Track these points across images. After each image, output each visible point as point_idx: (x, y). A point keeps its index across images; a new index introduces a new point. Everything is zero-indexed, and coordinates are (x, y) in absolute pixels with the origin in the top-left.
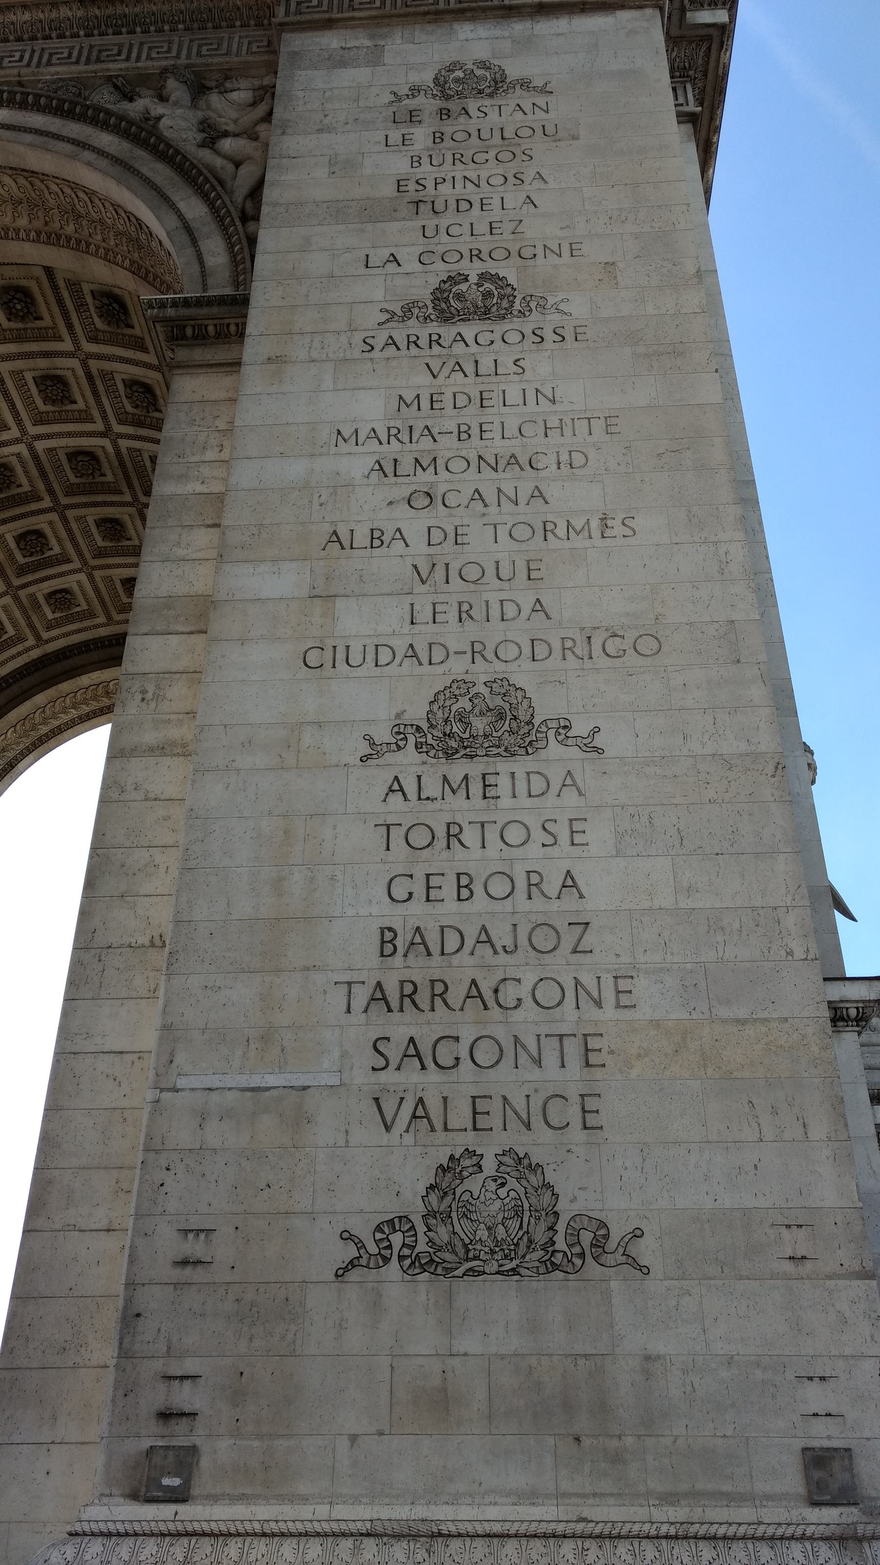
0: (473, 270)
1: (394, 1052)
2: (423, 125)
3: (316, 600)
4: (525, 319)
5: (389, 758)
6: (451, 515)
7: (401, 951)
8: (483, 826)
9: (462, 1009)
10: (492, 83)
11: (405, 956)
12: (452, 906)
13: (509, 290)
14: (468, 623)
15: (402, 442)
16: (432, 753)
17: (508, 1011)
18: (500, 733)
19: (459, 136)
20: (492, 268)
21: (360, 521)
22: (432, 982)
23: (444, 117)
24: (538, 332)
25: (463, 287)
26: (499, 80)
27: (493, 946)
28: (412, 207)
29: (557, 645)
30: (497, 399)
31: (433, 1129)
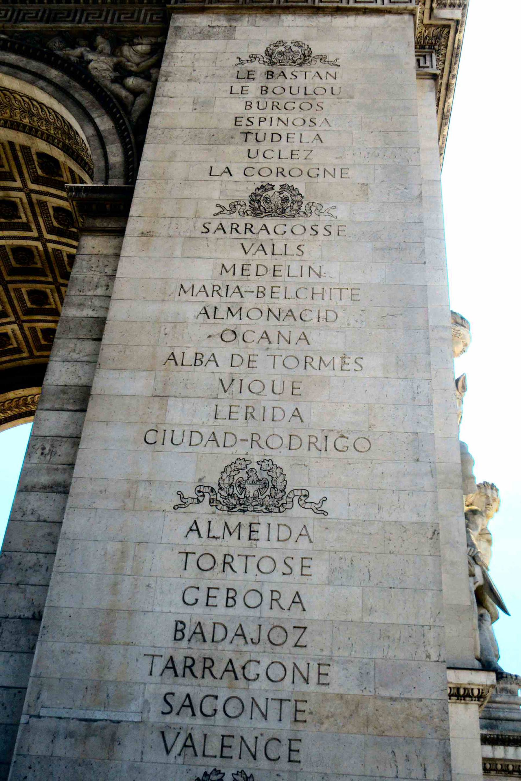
0: (278, 182)
1: (176, 703)
4: (308, 218)
5: (191, 508)
6: (247, 347)
7: (187, 637)
8: (247, 558)
9: (221, 678)
10: (302, 57)
11: (189, 640)
12: (221, 610)
13: (299, 198)
14: (250, 420)
15: (221, 296)
17: (250, 682)
18: (264, 496)
19: (278, 90)
20: (289, 181)
21: (189, 347)
23: (269, 77)
24: (314, 228)
25: (270, 193)
26: (306, 54)
28: (243, 136)
29: (305, 441)
30: (284, 272)
31: (196, 755)
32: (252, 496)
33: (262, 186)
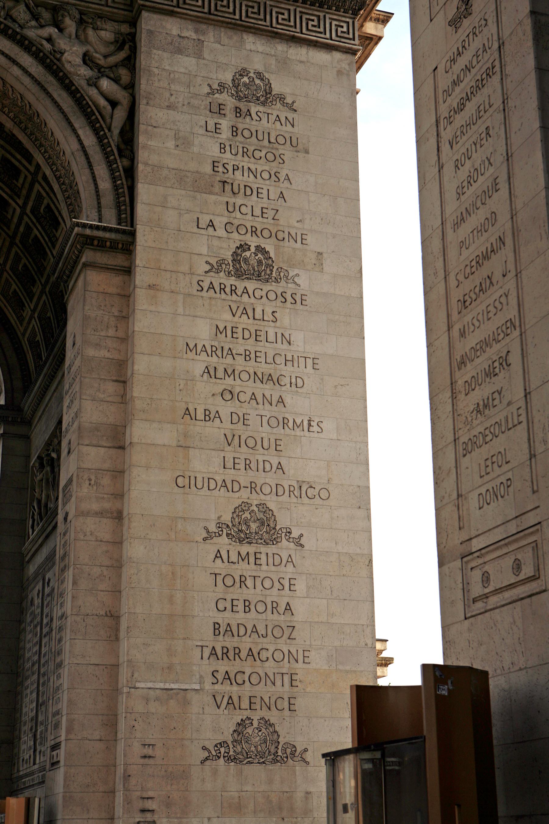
0: (253, 242)
1: (220, 677)
2: (226, 119)
3: (180, 448)
6: (241, 407)
7: (222, 634)
11: (224, 636)
12: (242, 614)
13: (270, 262)
14: (249, 471)
16: (234, 539)
18: (262, 533)
21: (199, 404)
22: (235, 648)
25: (248, 254)
26: (268, 91)
27: (258, 634)
28: (221, 184)
31: (235, 709)
32: (254, 531)
33: (241, 244)
